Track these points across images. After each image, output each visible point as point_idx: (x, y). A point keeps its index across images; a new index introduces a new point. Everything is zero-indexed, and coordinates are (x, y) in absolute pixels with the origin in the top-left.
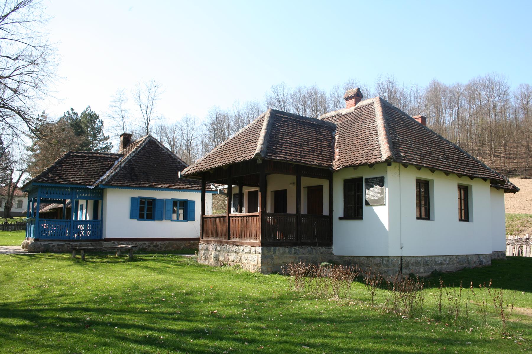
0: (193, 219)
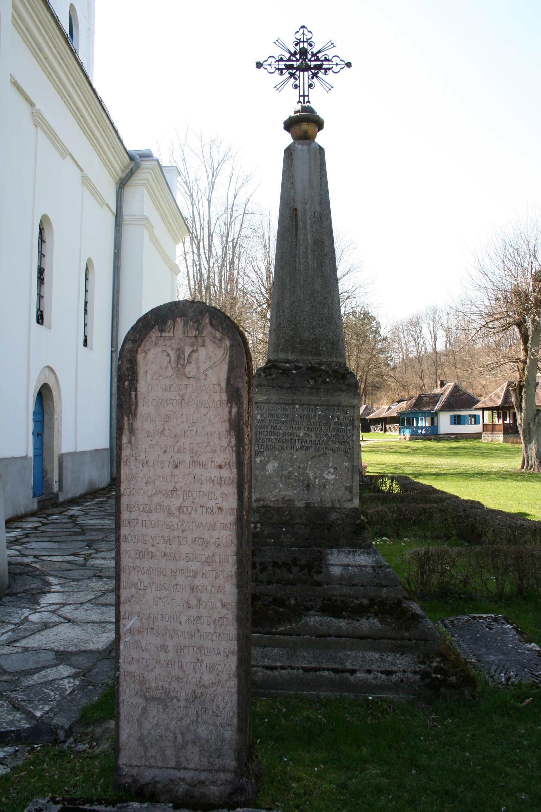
0: (479, 424)
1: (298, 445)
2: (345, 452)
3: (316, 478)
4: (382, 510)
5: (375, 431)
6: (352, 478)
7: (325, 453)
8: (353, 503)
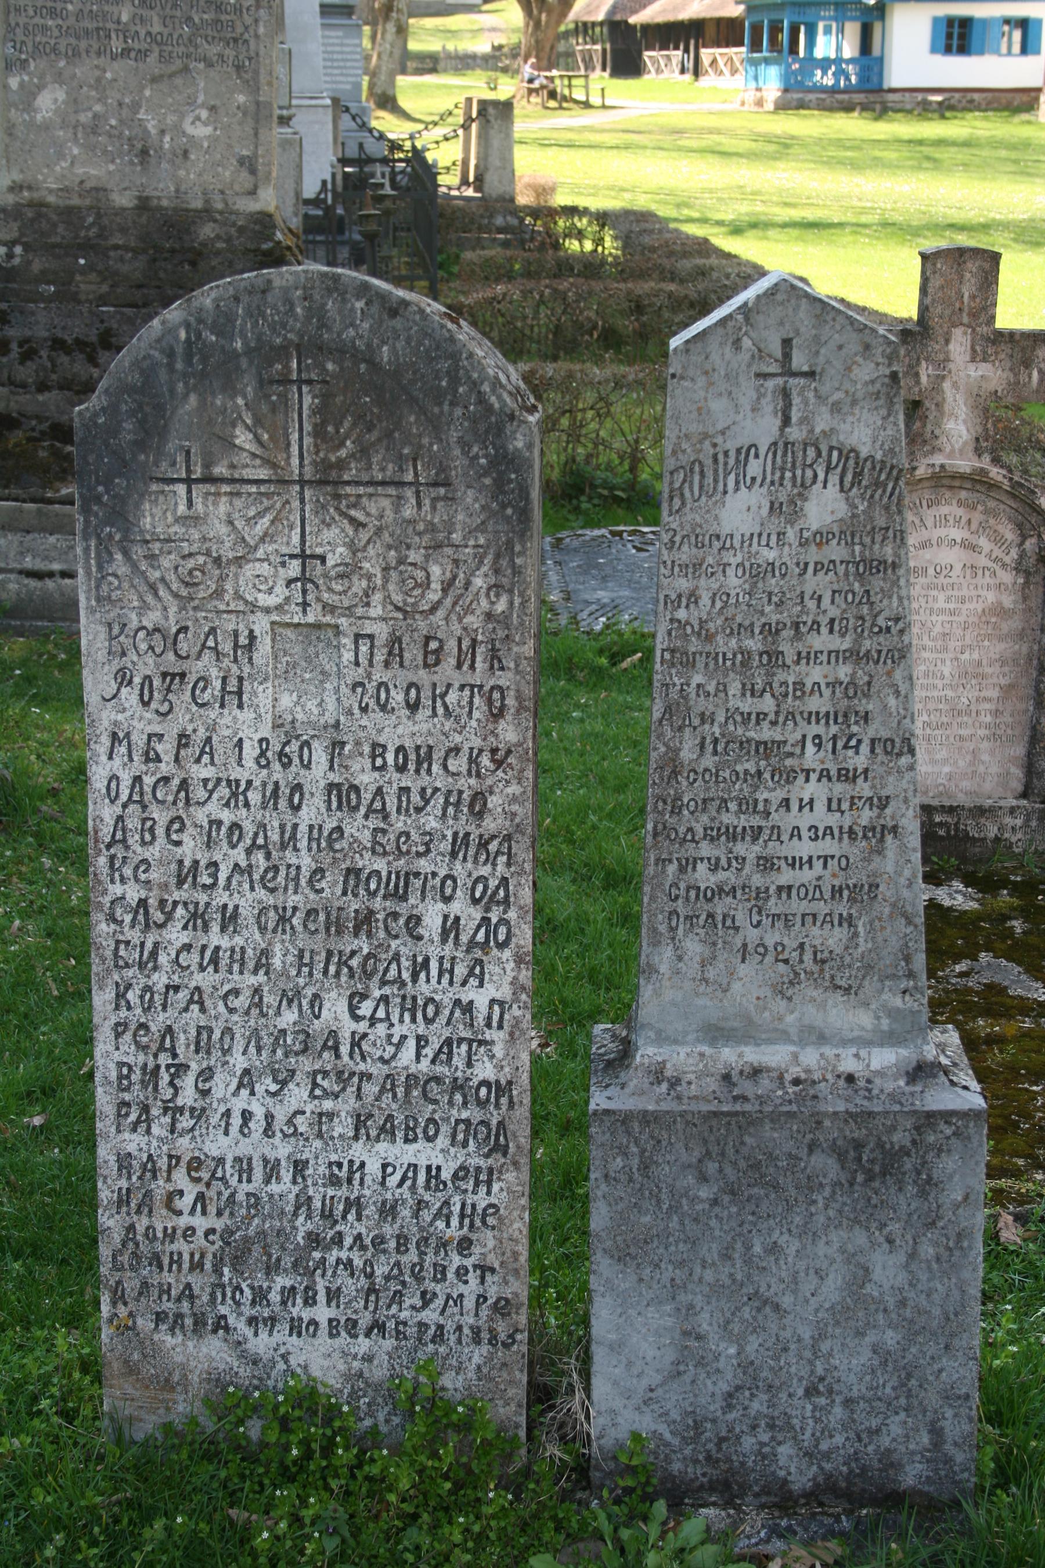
1: (116, 45)
2: (239, 68)
3: (163, 132)
4: (505, 295)
5: (659, 71)
6: (256, 134)
7: (186, 69)
8: (257, 200)
